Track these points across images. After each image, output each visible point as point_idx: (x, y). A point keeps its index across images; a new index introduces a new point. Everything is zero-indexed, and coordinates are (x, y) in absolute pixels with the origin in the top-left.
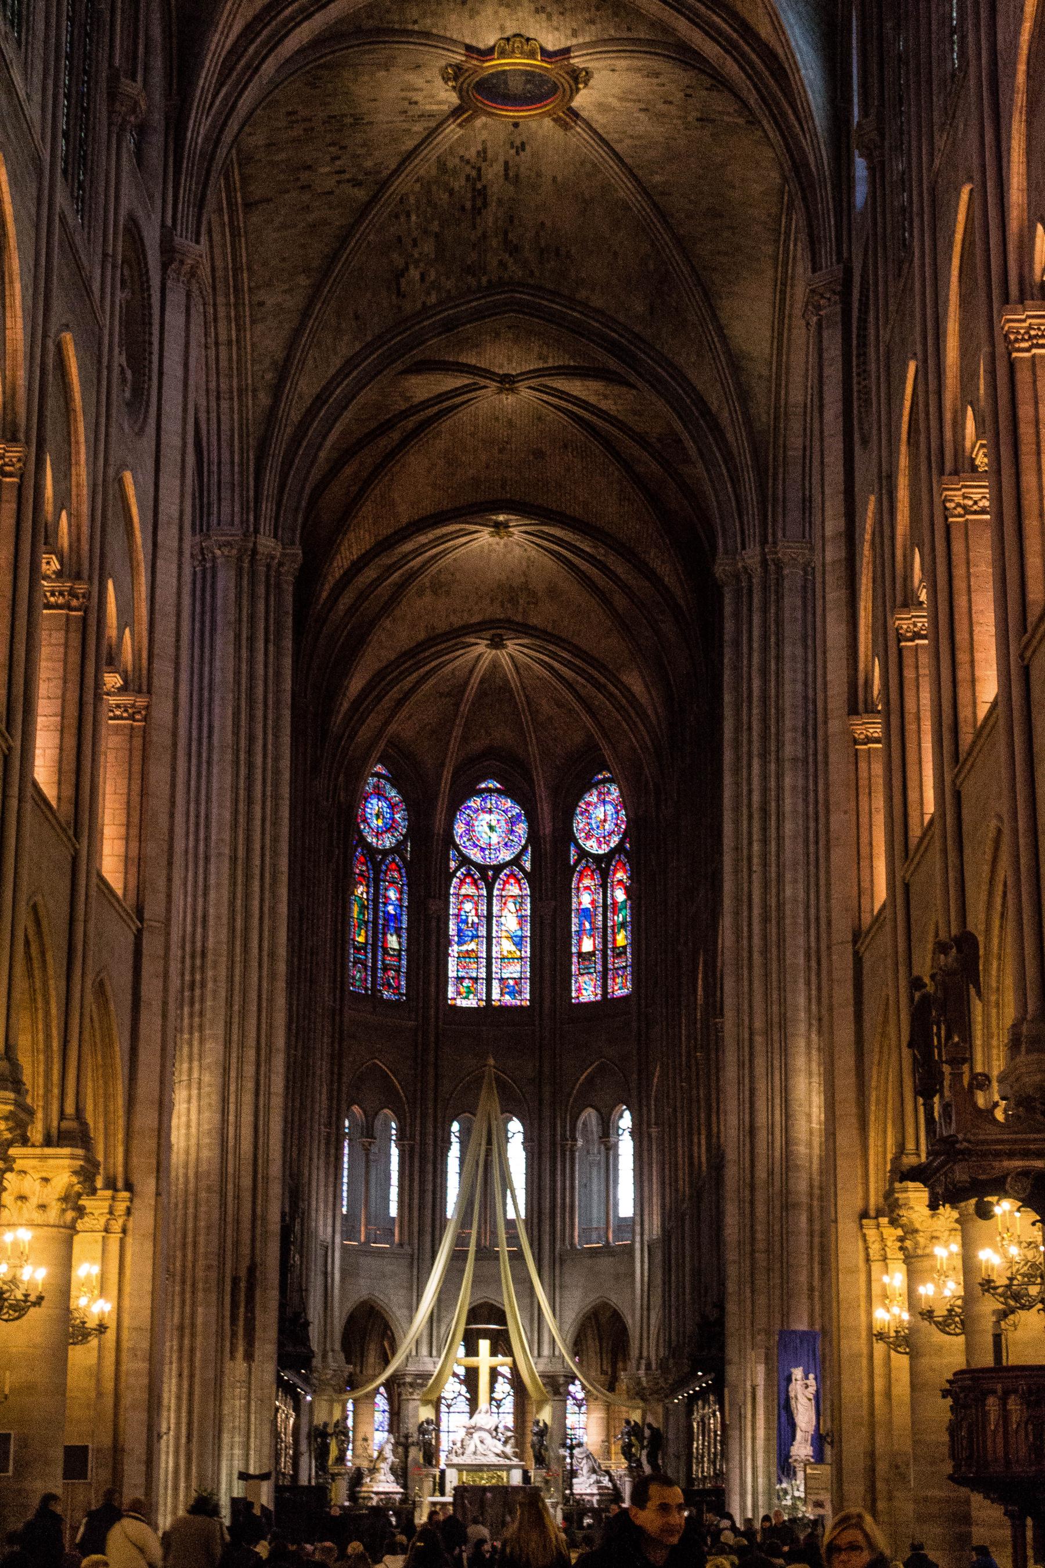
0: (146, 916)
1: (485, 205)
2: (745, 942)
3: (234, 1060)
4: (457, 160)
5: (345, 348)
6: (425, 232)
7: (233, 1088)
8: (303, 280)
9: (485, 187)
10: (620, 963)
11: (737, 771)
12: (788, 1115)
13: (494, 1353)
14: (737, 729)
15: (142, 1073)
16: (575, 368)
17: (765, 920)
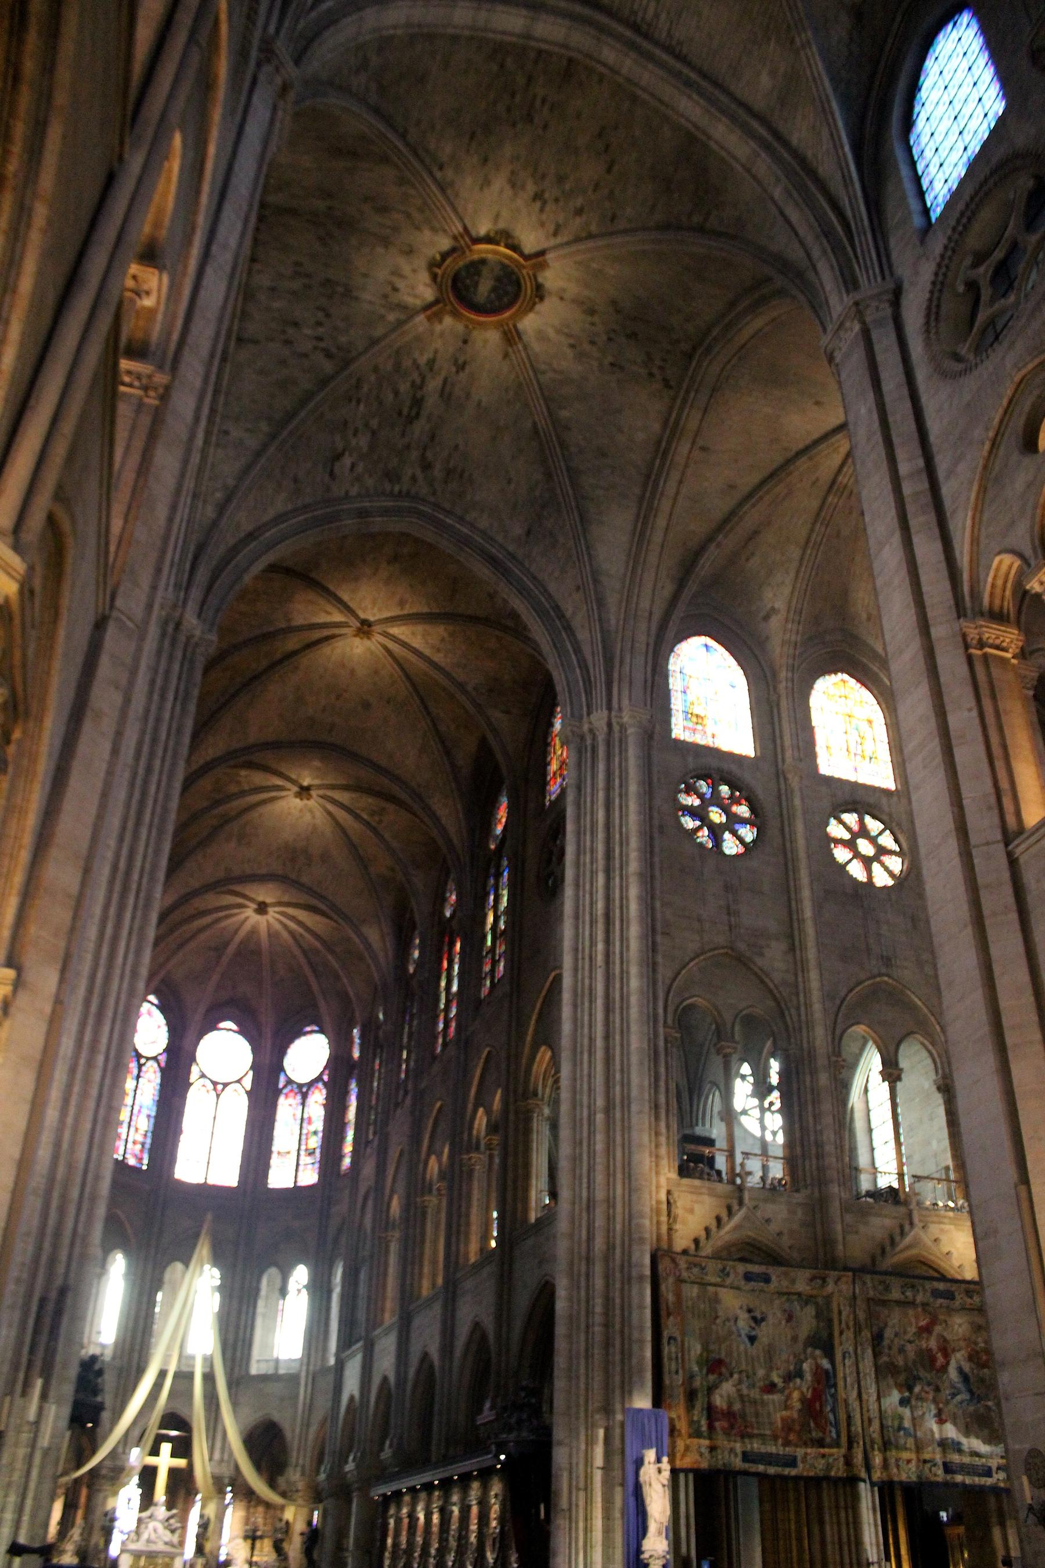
0: (119, 602)
1: (418, 415)
2: (586, 1030)
3: (82, 1062)
4: (409, 363)
5: (280, 504)
6: (367, 425)
7: (76, 1089)
8: (264, 426)
9: (422, 399)
10: (309, 1160)
11: (577, 885)
12: (631, 1189)
13: (173, 1455)
14: (578, 853)
15: (69, 805)
16: (427, 614)
17: (608, 1009)
